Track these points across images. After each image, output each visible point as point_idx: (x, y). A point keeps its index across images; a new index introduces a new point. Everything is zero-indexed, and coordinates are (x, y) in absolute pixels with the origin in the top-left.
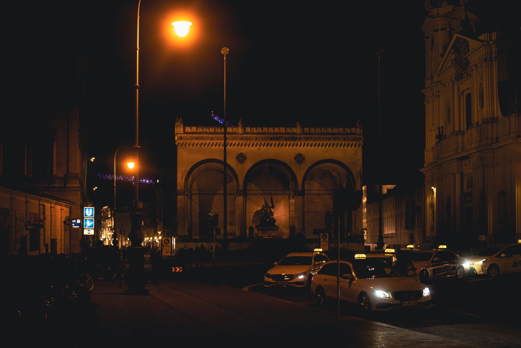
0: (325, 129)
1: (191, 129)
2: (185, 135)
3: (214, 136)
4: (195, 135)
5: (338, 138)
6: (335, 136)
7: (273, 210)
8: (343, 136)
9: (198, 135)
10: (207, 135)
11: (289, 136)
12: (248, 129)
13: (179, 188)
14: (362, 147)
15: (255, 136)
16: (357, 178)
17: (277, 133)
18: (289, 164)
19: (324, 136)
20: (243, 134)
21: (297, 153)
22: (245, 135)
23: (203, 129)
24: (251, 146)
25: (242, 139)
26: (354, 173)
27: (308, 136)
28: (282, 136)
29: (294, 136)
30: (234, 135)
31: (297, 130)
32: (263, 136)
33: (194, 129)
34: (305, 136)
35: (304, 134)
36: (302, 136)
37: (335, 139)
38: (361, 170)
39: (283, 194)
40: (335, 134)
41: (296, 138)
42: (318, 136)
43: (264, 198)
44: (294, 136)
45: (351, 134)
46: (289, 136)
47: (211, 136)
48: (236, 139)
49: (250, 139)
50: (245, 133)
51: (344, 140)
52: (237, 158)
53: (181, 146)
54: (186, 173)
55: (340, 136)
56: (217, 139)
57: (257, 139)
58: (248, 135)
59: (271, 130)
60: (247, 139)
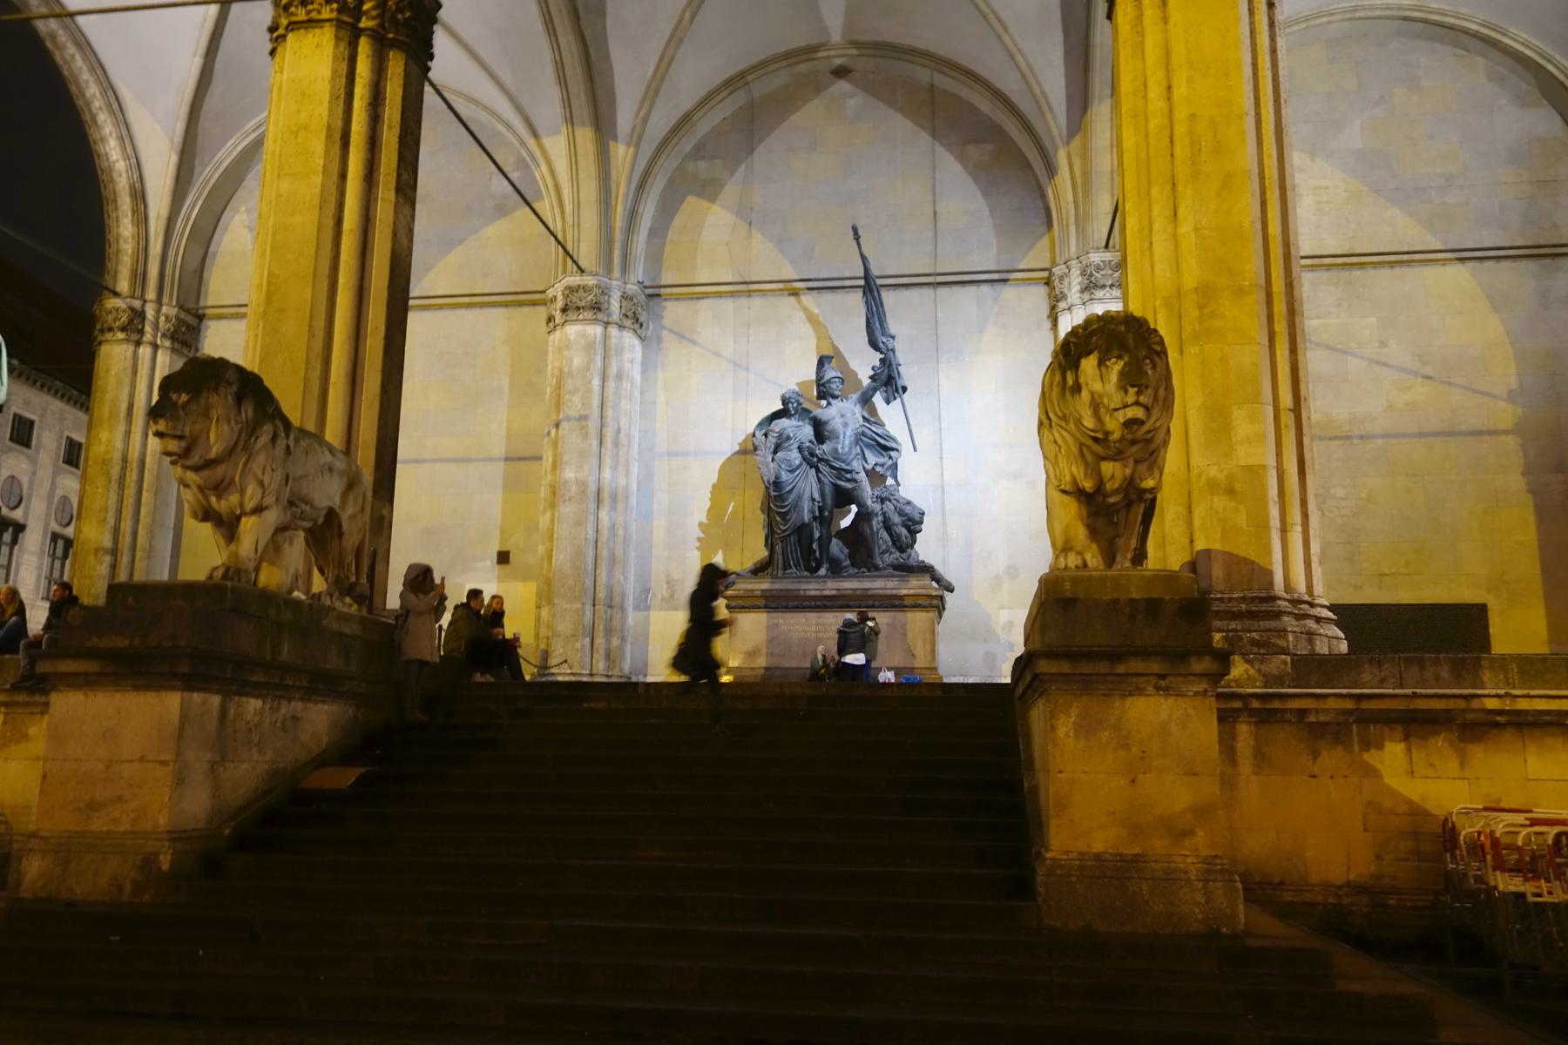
7: (890, 415)
39: (1000, 278)
43: (812, 320)
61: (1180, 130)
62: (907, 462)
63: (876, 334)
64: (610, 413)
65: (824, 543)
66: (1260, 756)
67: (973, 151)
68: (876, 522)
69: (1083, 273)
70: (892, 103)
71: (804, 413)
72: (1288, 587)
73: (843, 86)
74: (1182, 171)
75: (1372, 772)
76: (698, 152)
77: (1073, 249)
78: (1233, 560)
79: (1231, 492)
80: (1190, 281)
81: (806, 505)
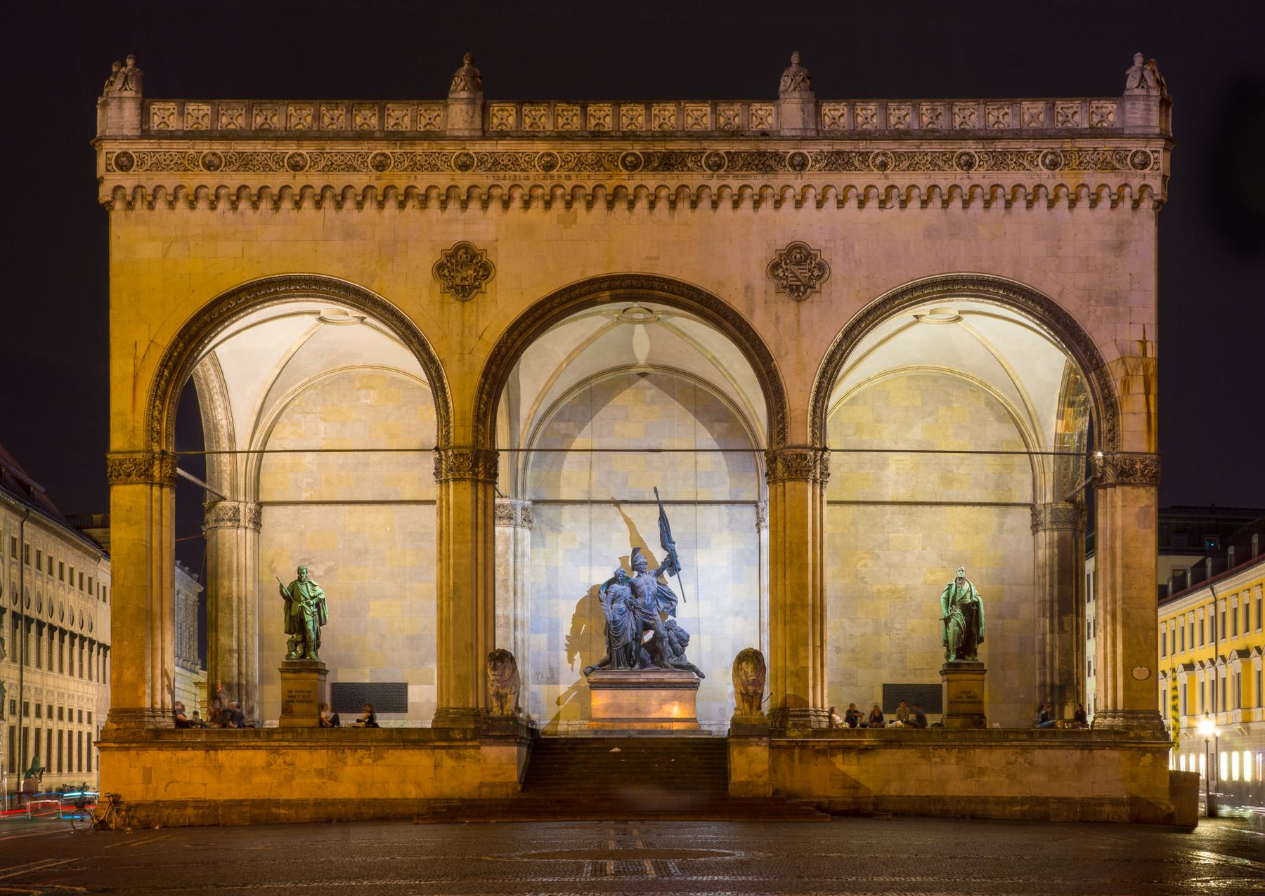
0: (941, 109)
1: (182, 113)
2: (145, 146)
3: (307, 149)
4: (205, 148)
5: (1021, 154)
6: (999, 146)
8: (1046, 146)
9: (218, 147)
12: (504, 115)
13: (117, 442)
14: (1159, 205)
15: (541, 147)
16: (1126, 384)
17: (666, 136)
19: (937, 147)
20: (471, 139)
21: (782, 243)
22: (488, 147)
23: (216, 116)
24: (516, 204)
25: (464, 167)
26: (1109, 354)
27: (847, 147)
28: (696, 146)
29: (763, 146)
30: (420, 148)
31: (787, 112)
32: (585, 147)
33: (199, 113)
34: (825, 147)
35: (821, 135)
36: (809, 149)
37: (999, 161)
38: (1152, 336)
40: (1000, 135)
42: (906, 147)
45: (1096, 133)
47: (290, 148)
48: (434, 168)
49: (514, 163)
50: (485, 135)
53: (130, 205)
55: (1030, 146)
56: (330, 168)
57: (549, 167)
58: (501, 147)
59: (635, 116)
60: (494, 164)
62: (681, 608)
63: (666, 539)
64: (519, 577)
65: (637, 652)
66: (801, 759)
67: (718, 427)
68: (666, 642)
70: (672, 394)
72: (814, 706)
73: (644, 382)
74: (788, 562)
75: (833, 764)
76: (559, 418)
78: (796, 697)
79: (797, 675)
80: (788, 602)
81: (629, 633)
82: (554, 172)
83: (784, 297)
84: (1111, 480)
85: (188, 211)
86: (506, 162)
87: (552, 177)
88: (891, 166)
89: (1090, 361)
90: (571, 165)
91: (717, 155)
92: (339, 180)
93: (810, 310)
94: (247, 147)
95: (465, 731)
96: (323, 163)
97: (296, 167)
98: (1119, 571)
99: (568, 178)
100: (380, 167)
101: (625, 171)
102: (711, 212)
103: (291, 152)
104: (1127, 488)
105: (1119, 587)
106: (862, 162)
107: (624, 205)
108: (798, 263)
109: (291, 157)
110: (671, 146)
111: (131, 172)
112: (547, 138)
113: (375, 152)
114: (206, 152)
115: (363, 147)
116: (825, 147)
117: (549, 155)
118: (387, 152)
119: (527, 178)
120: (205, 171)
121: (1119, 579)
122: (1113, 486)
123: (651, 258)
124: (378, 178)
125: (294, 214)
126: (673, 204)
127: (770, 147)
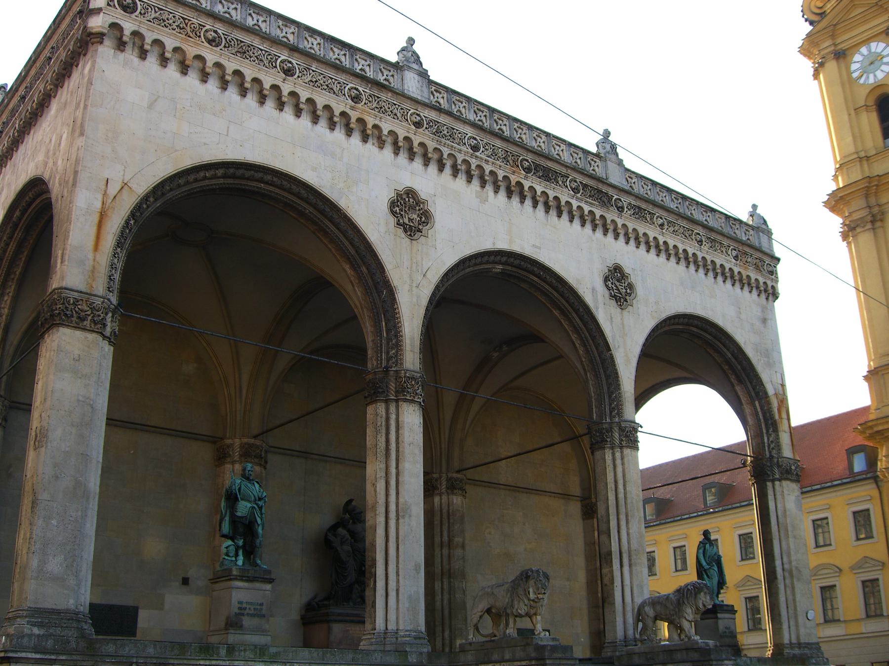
3: (296, 61)
4: (209, 24)
6: (713, 236)
8: (733, 244)
9: (221, 29)
10: (265, 46)
11: (586, 181)
15: (470, 131)
17: (548, 157)
18: (588, 299)
19: (684, 223)
21: (610, 263)
25: (418, 125)
26: (771, 391)
27: (643, 205)
29: (601, 187)
32: (498, 143)
36: (626, 200)
41: (610, 198)
44: (601, 187)
46: (586, 181)
51: (736, 258)
52: (393, 204)
54: (128, 203)
55: (726, 242)
56: (314, 83)
57: (475, 148)
61: (629, 501)
69: (449, 480)
71: (344, 527)
77: (444, 469)
82: (478, 154)
83: (613, 302)
84: (777, 476)
85: (177, 75)
86: (445, 132)
87: (476, 157)
88: (666, 227)
89: (757, 394)
90: (490, 152)
91: (576, 181)
92: (322, 99)
93: (628, 317)
94: (247, 39)
95: (421, 653)
96: (309, 79)
97: (288, 72)
98: (791, 540)
99: (487, 162)
100: (356, 99)
101: (523, 172)
102: (569, 223)
103: (283, 57)
104: (788, 482)
105: (792, 553)
106: (651, 219)
107: (518, 199)
108: (618, 281)
109: (283, 62)
110: (550, 164)
111: (133, 16)
112: (473, 125)
113: (351, 85)
114: (208, 27)
115: (342, 78)
116: (633, 202)
117: (475, 139)
118: (360, 89)
119: (460, 151)
120: (206, 44)
121: (792, 547)
122: (780, 480)
123: (536, 247)
124: (352, 108)
125: (276, 113)
126: (547, 208)
127: (604, 189)
